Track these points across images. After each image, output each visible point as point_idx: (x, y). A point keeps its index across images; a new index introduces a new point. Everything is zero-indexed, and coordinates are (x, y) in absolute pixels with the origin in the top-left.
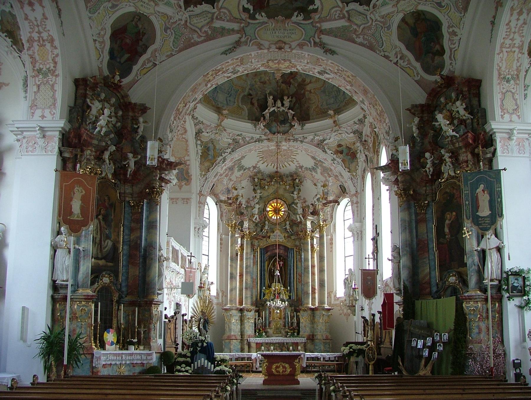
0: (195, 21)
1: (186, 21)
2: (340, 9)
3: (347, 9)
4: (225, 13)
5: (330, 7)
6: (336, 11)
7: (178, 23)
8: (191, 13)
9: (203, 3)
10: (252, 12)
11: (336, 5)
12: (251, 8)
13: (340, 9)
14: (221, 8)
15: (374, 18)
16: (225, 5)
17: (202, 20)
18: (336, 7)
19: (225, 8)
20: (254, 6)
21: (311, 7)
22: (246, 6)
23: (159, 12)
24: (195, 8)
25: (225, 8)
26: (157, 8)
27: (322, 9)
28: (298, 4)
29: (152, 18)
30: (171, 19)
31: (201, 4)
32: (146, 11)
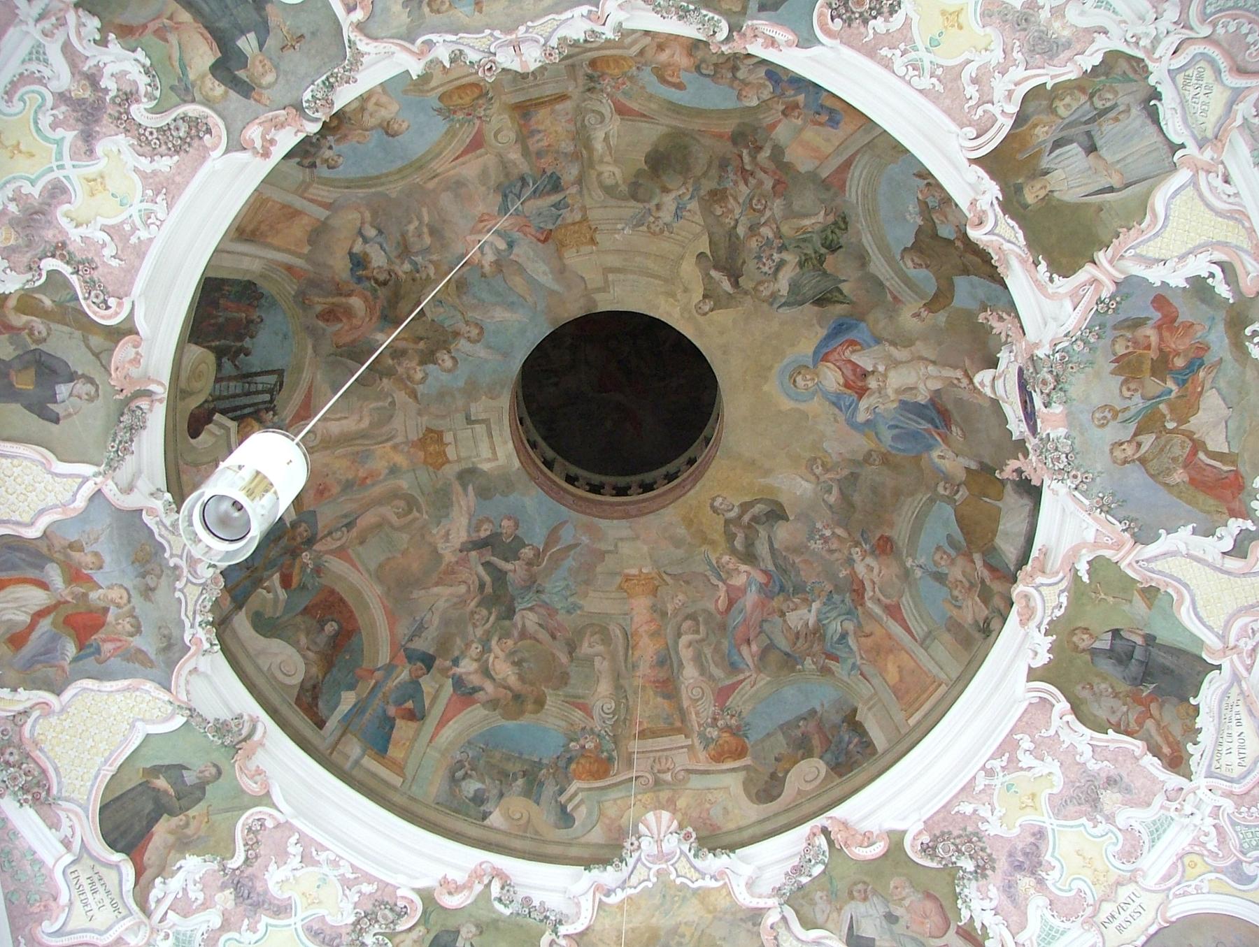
0: (1234, 759)
1: (1229, 795)
2: (1202, 175)
3: (1191, 149)
4: (1244, 633)
5: (1209, 215)
6: (1212, 189)
7: (1224, 823)
8: (1205, 761)
9: (1193, 701)
10: (1249, 525)
11: (1190, 190)
12: (1235, 525)
13: (1202, 175)
14: (1223, 637)
15: (1174, 40)
16: (1218, 624)
17: (1235, 731)
18: (1198, 190)
19: (1228, 625)
20: (1234, 514)
21: (1223, 290)
22: (1228, 544)
23: (1167, 877)
24: (1200, 738)
25: (1228, 625)
26: (1151, 881)
27: (1223, 245)
28: (1218, 340)
29: (1179, 908)
30: (1203, 844)
31: (1196, 709)
32: (1142, 921)
